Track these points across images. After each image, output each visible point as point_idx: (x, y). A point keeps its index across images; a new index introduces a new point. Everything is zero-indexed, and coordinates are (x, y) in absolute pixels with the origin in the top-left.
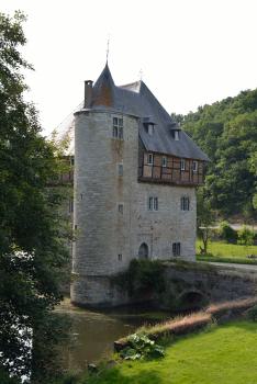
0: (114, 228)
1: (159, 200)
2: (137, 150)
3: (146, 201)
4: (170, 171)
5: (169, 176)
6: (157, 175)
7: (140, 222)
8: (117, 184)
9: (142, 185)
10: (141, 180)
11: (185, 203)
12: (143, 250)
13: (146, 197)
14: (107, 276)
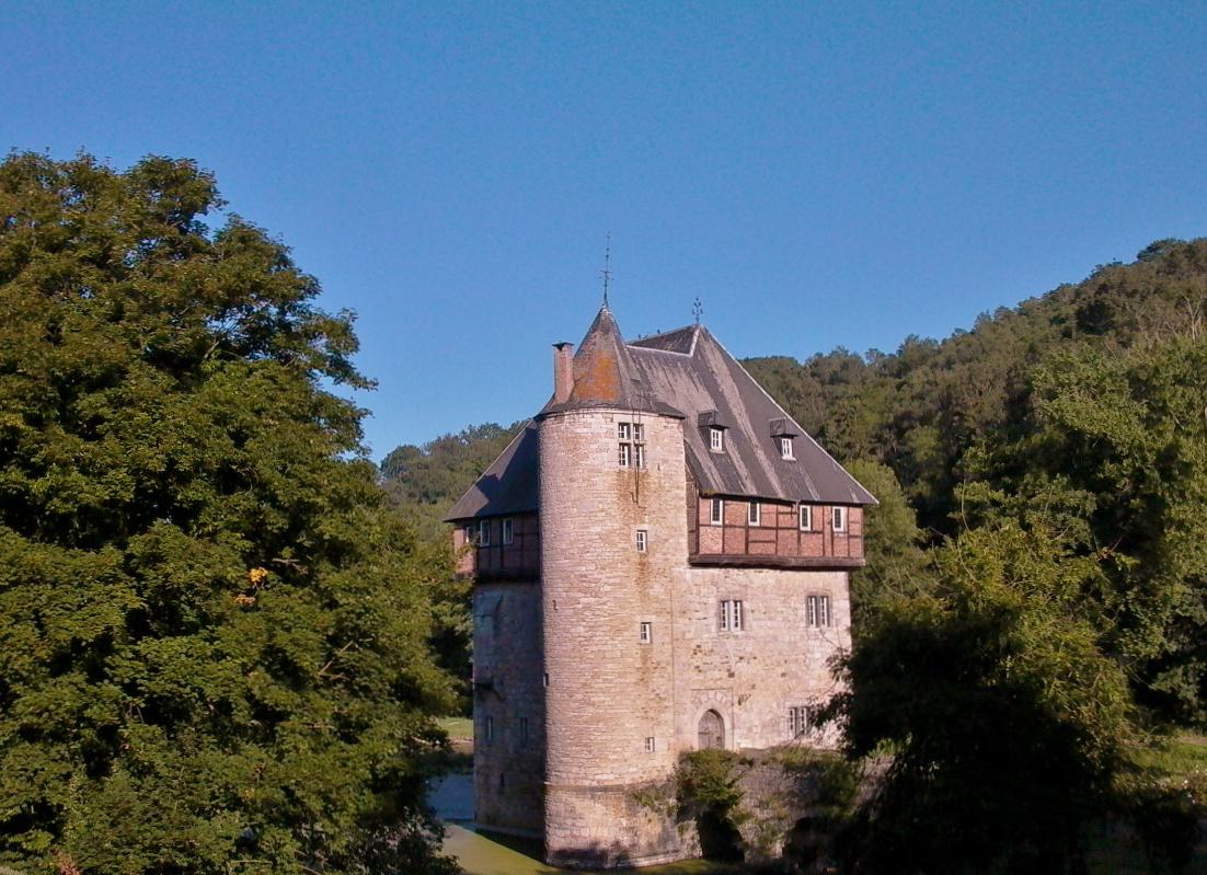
0: (632, 679)
1: (746, 605)
2: (683, 493)
3: (712, 612)
4: (772, 535)
5: (770, 549)
6: (737, 547)
7: (697, 661)
8: (635, 575)
9: (699, 571)
10: (699, 562)
11: (817, 606)
12: (711, 726)
13: (712, 601)
14: (619, 788)
